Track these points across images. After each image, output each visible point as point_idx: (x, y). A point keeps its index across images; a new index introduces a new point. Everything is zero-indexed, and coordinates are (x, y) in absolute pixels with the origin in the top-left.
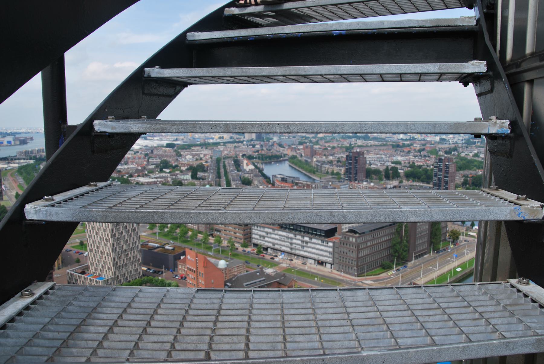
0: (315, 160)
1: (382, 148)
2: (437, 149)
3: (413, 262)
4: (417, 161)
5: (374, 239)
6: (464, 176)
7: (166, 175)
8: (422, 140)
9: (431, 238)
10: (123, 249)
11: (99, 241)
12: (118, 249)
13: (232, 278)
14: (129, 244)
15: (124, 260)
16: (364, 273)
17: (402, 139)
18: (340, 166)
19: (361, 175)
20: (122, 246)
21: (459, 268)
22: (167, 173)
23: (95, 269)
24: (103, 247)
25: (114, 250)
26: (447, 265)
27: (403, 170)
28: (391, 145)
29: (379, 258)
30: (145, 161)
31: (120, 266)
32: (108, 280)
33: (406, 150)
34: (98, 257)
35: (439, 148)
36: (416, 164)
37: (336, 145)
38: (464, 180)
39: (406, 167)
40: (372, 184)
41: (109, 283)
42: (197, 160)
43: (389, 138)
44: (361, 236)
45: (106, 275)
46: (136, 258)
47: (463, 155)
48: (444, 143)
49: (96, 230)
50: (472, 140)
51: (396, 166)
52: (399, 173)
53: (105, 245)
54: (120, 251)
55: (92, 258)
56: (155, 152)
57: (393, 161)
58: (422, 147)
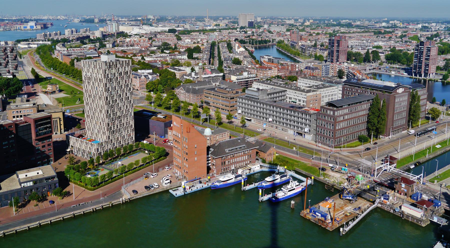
0: (300, 44)
1: (364, 34)
2: (419, 35)
3: (390, 137)
4: (398, 46)
5: (351, 113)
6: (446, 59)
7: (166, 55)
8: (403, 28)
9: (409, 115)
10: (116, 115)
11: (95, 108)
12: (112, 115)
13: (215, 144)
14: (123, 111)
15: (117, 126)
16: (341, 144)
17: (384, 27)
18: (323, 50)
19: (343, 58)
20: (116, 113)
21: (439, 145)
22: (167, 53)
23: (92, 134)
24: (98, 113)
25: (108, 116)
26: (426, 141)
27: (383, 53)
28: (373, 31)
29: (357, 132)
30: (148, 43)
31: (113, 131)
32: (102, 143)
33: (387, 37)
34: (94, 122)
35: (421, 35)
36: (397, 48)
37: (320, 32)
38: (446, 63)
39: (387, 51)
40: (353, 65)
41: (103, 147)
42: (194, 43)
43: (371, 26)
44: (339, 110)
45: (101, 139)
46: (130, 124)
47: (445, 41)
48: (426, 30)
49: (93, 98)
51: (377, 50)
52: (380, 56)
53: (101, 111)
54: (114, 117)
55: (89, 123)
56: (158, 36)
57: (374, 45)
58: (404, 34)
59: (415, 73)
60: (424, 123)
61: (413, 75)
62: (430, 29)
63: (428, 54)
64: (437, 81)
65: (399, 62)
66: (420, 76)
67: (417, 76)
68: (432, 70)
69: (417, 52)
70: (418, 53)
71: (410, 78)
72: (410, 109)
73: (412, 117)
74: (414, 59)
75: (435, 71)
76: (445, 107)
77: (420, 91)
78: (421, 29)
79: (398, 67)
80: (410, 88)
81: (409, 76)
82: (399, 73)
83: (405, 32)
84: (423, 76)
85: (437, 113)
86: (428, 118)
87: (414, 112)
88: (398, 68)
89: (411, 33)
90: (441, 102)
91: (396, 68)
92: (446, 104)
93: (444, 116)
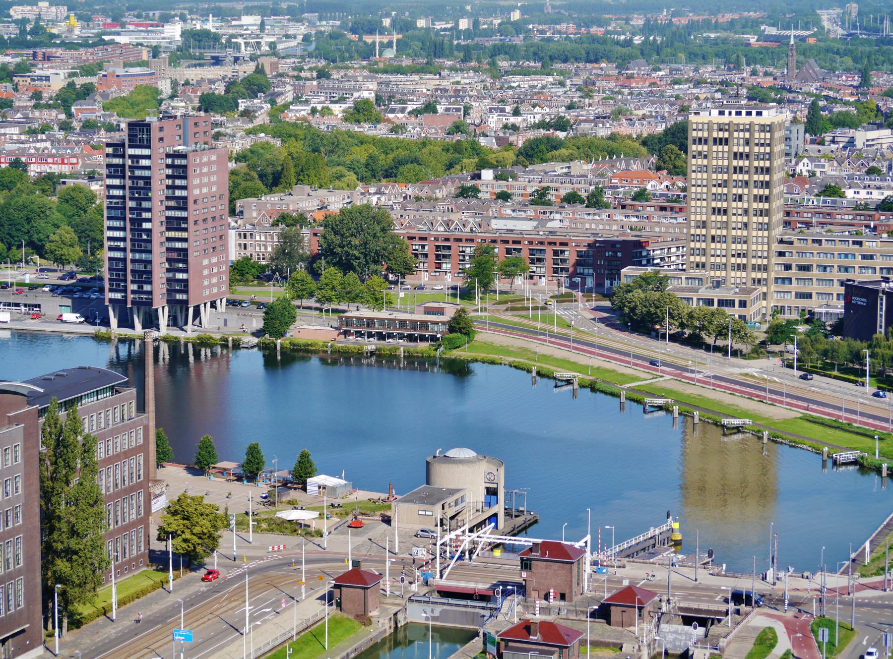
2: (165, 87)
4: (42, 158)
6: (283, 218)
8: (85, 45)
9: (49, 553)
35: (174, 84)
36: (34, 170)
38: (284, 236)
48: (209, 54)
50: (354, 37)
58: (80, 81)
59: (118, 304)
60: (144, 592)
61: (114, 321)
62: (230, 51)
63: (178, 193)
64: (237, 346)
65: (40, 250)
66: (151, 322)
67: (132, 327)
68: (211, 286)
69: (116, 182)
70: (123, 187)
71: (97, 338)
72: (49, 519)
73: (62, 565)
74: (107, 223)
75: (224, 288)
76: (262, 488)
77: (105, 406)
78: (179, 49)
79: (27, 279)
80: (31, 398)
81: (90, 329)
82: (37, 316)
83: (88, 71)
84: (163, 321)
85: (204, 525)
86: (158, 560)
87: (73, 532)
88: (33, 287)
89: (120, 71)
90: (244, 458)
91: (21, 284)
92: (266, 468)
93: (251, 536)
